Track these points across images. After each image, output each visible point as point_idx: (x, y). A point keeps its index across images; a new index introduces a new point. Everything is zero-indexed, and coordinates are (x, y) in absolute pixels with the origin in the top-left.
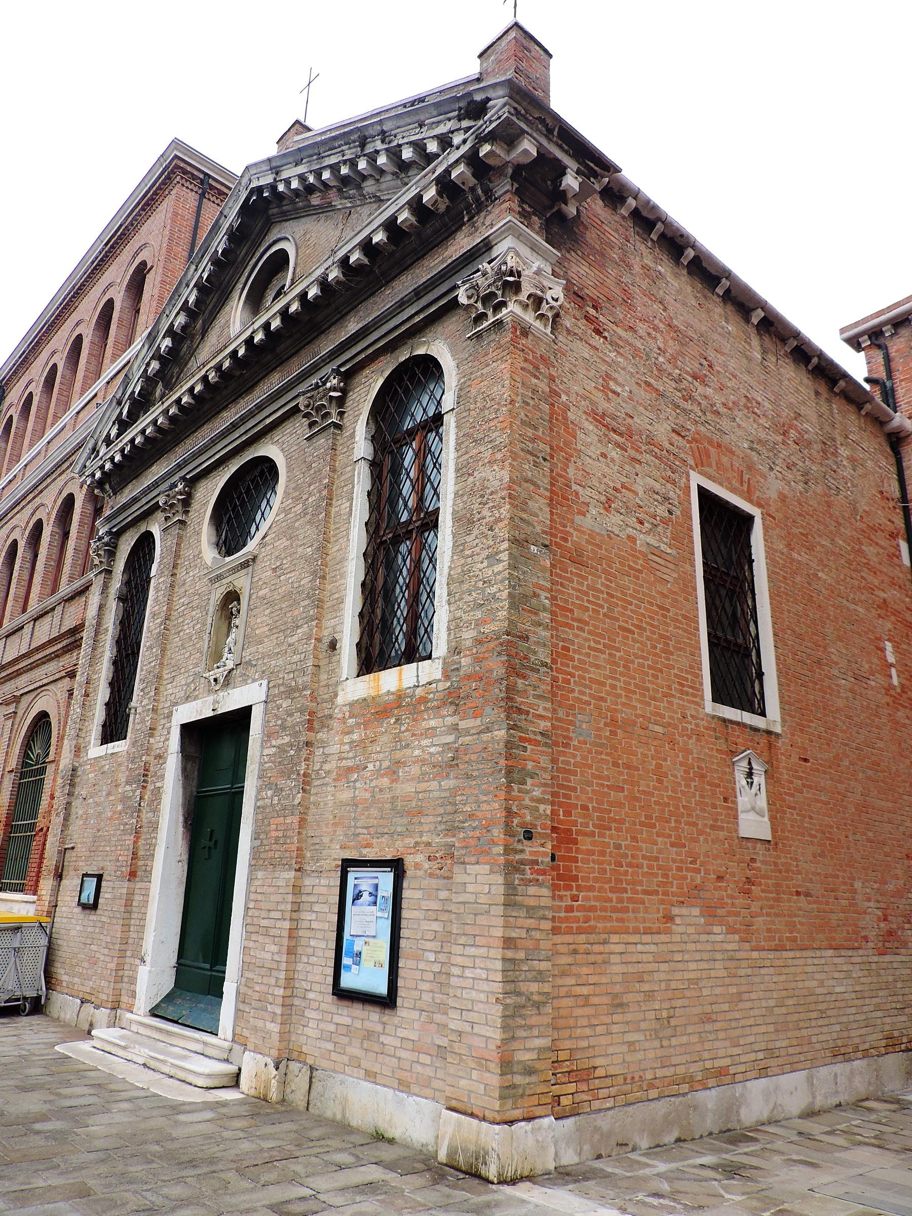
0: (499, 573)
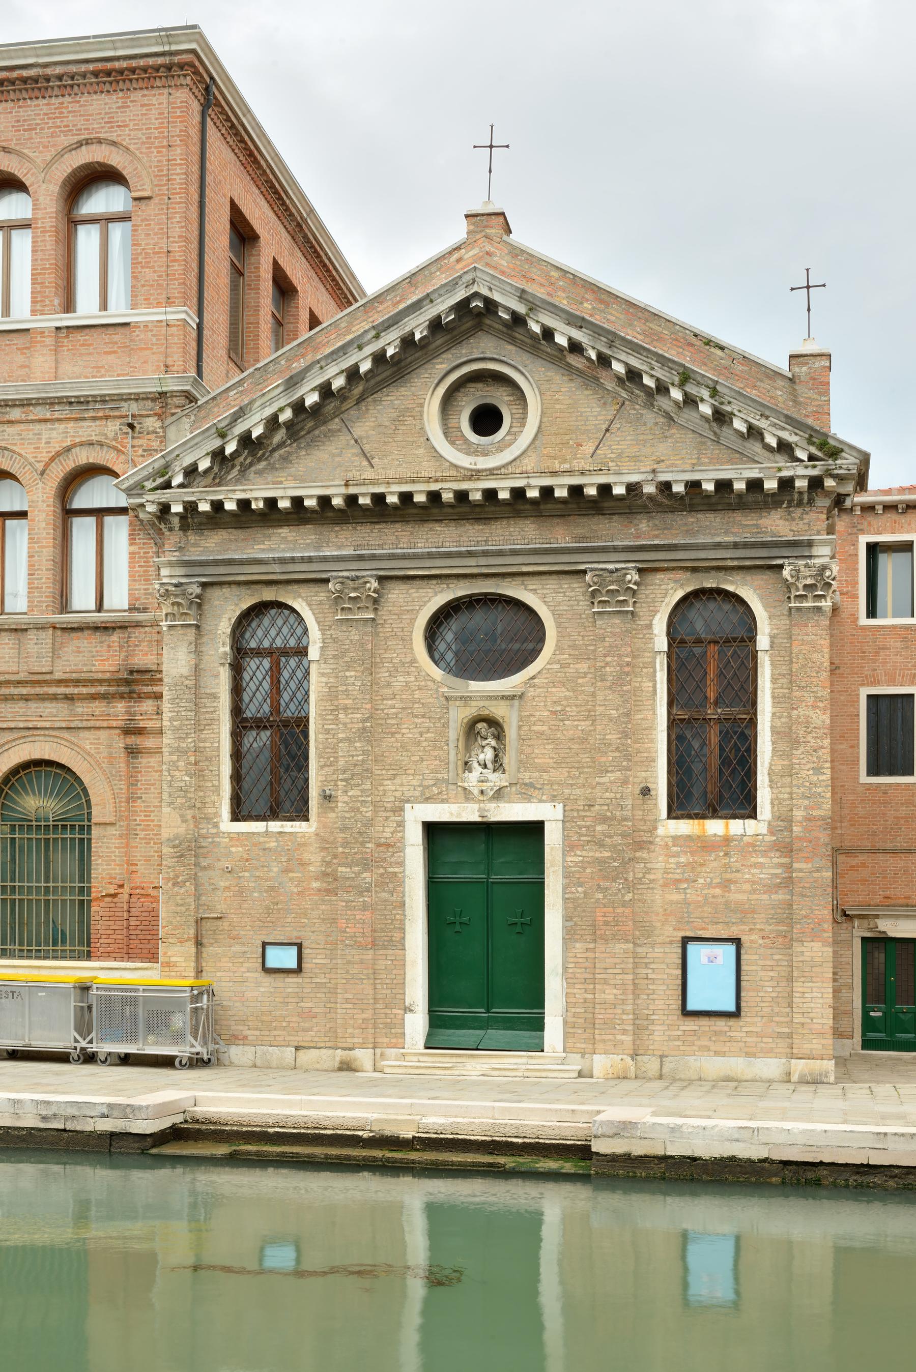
0: (823, 781)
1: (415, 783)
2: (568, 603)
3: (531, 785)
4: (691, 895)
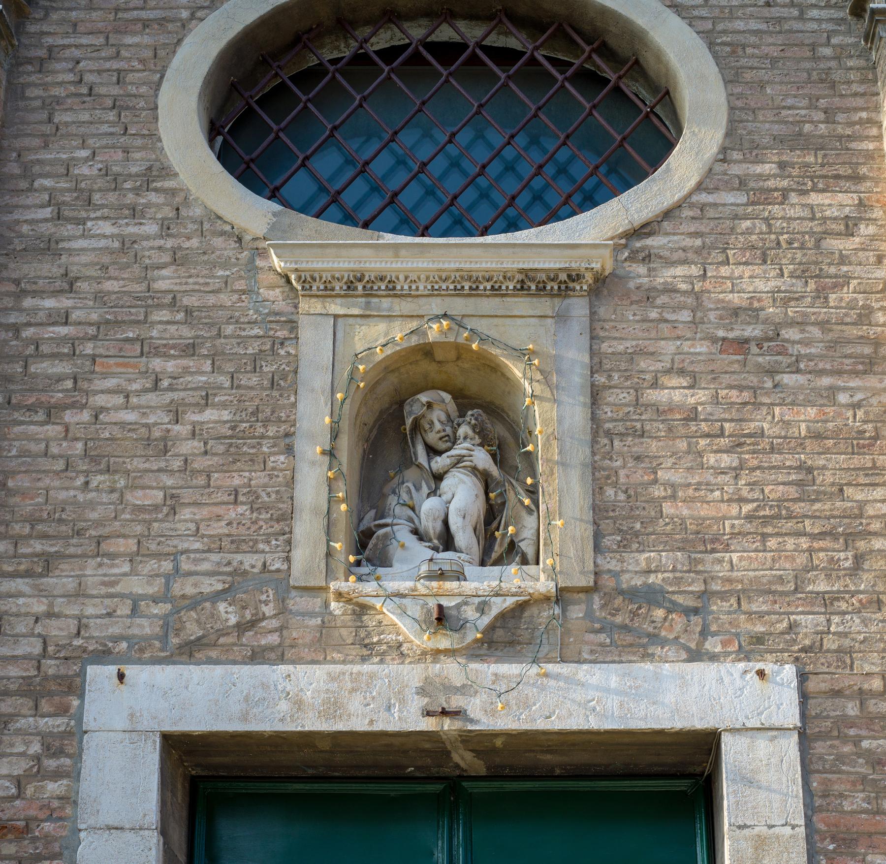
1: (137, 586)
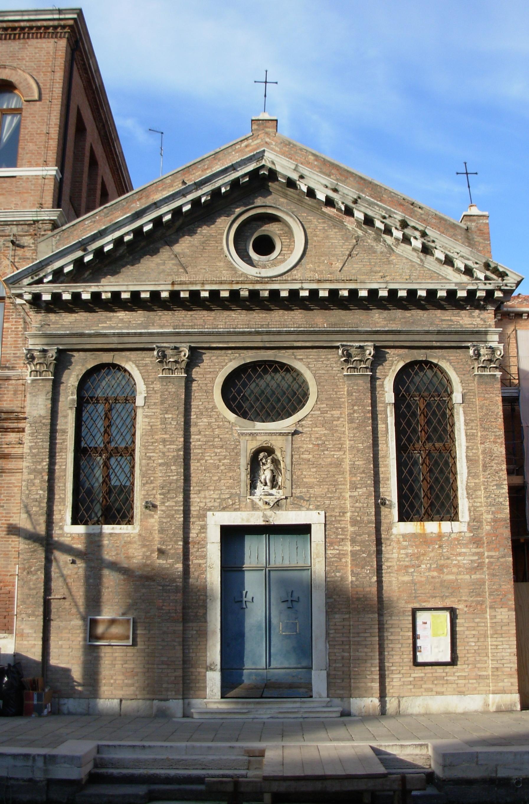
0: (503, 493)
1: (215, 496)
2: (326, 369)
3: (301, 498)
4: (417, 577)
